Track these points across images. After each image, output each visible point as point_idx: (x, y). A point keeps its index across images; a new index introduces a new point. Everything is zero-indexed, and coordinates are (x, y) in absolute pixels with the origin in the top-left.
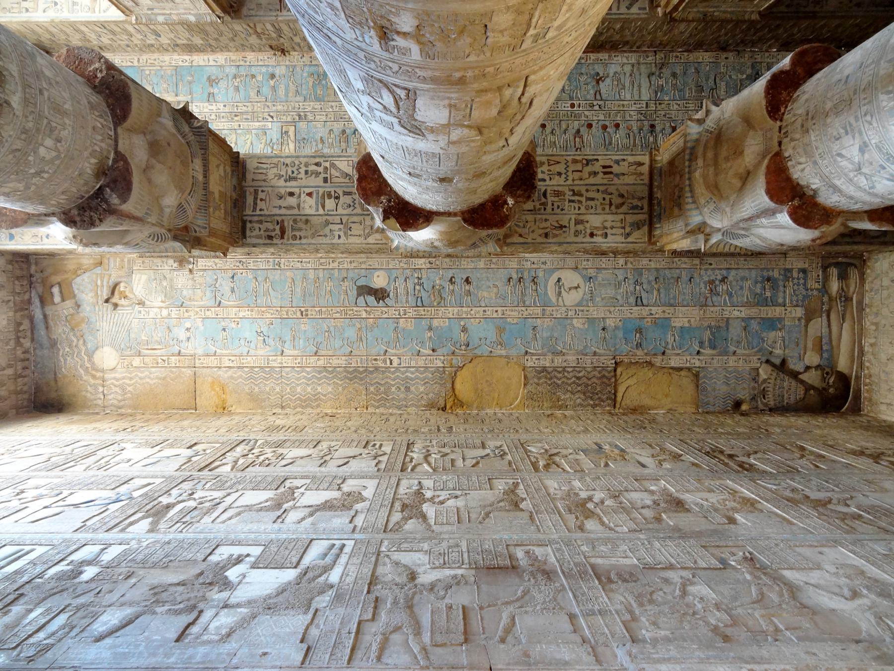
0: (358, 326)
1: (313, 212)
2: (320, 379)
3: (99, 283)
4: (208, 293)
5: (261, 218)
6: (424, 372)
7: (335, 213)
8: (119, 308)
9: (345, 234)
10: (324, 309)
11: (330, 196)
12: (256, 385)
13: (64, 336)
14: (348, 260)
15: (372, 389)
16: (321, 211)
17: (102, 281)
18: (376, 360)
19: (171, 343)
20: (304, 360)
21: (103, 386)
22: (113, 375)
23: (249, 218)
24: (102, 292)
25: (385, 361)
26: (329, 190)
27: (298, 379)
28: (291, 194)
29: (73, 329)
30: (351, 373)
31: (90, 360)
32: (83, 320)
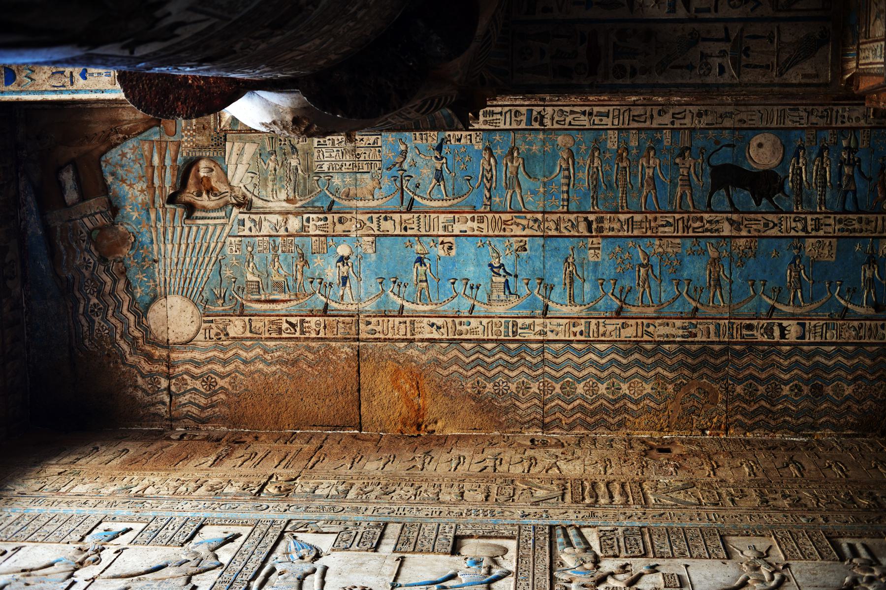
0: (712, 253)
2: (626, 367)
3: (156, 161)
4: (386, 183)
8: (198, 214)
10: (638, 217)
12: (487, 378)
13: (87, 274)
14: (695, 109)
15: (739, 389)
17: (162, 159)
18: (750, 327)
19: (308, 288)
20: (593, 326)
21: (169, 377)
22: (188, 355)
24: (163, 180)
27: (579, 367)
29: (103, 260)
30: (694, 355)
31: (139, 323)
32: (124, 239)
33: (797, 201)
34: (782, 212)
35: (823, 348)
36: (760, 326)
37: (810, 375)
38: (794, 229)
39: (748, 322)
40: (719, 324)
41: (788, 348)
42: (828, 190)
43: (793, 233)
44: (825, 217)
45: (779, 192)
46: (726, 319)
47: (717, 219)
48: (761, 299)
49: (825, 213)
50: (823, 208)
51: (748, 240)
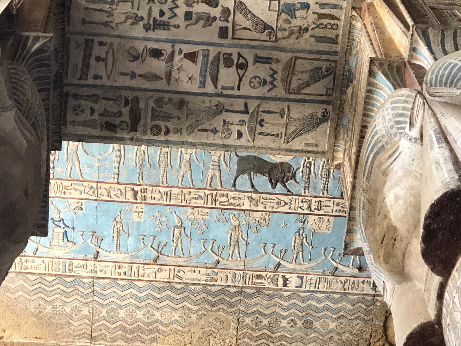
1: (194, 88)
2: (160, 300)
5: (94, 91)
6: (341, 300)
7: (235, 92)
9: (252, 131)
10: (175, 191)
11: (228, 62)
16: (210, 88)
18: (259, 277)
23: (72, 90)
25: (274, 281)
26: (228, 51)
27: (122, 298)
28: (156, 53)
30: (214, 295)
33: (305, 187)
34: (292, 194)
35: (315, 294)
36: (268, 276)
37: (304, 313)
38: (300, 208)
39: (259, 273)
40: (235, 274)
41: (289, 293)
42: (330, 180)
43: (300, 211)
44: (326, 201)
45: (291, 179)
46: (241, 270)
47: (239, 196)
48: (270, 258)
49: (326, 197)
50: (325, 194)
51: (264, 213)
